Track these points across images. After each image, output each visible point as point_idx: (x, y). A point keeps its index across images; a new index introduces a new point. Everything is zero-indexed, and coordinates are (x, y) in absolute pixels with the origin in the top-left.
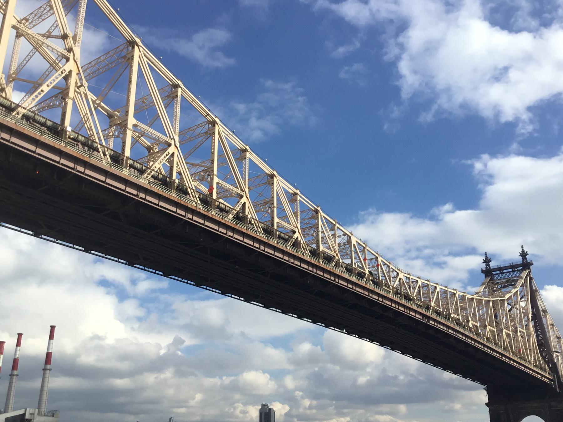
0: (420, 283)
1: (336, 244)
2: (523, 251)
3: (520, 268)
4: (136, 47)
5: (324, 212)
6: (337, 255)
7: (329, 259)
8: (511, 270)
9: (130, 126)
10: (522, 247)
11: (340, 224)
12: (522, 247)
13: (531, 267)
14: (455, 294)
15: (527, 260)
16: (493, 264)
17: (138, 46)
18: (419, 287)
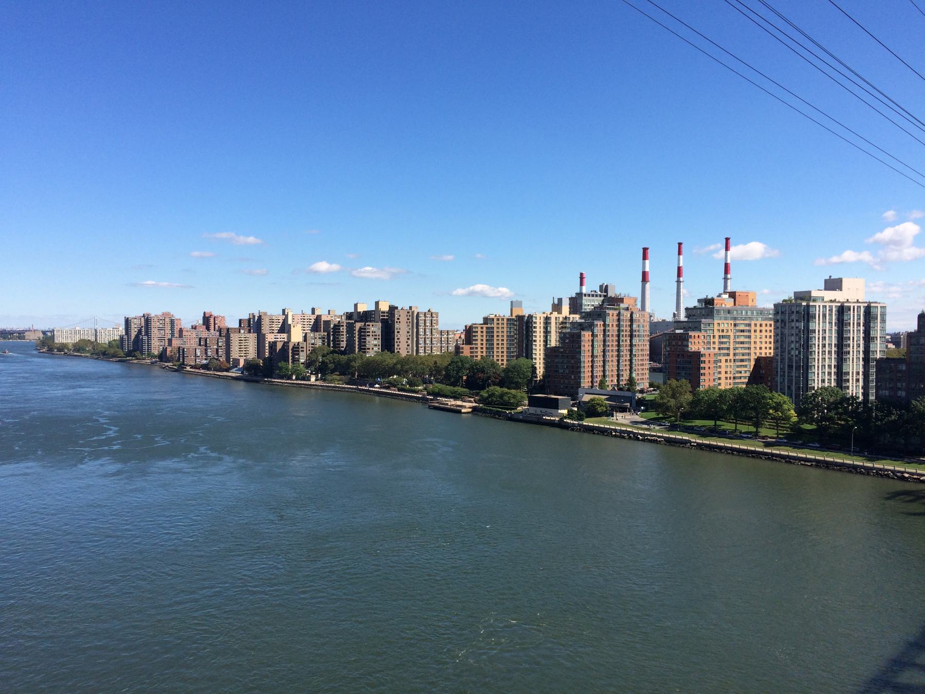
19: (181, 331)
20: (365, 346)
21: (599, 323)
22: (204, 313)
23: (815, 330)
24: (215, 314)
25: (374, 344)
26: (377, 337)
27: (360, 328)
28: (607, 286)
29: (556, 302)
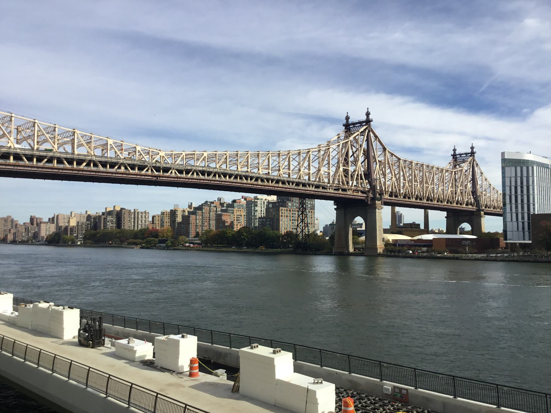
3: (364, 124)
8: (359, 125)
10: (368, 109)
12: (368, 109)
19: (16, 225)
20: (106, 227)
21: (200, 212)
22: (31, 216)
23: (257, 211)
24: (37, 216)
25: (111, 225)
26: (113, 223)
27: (104, 218)
28: (220, 199)
29: (190, 204)
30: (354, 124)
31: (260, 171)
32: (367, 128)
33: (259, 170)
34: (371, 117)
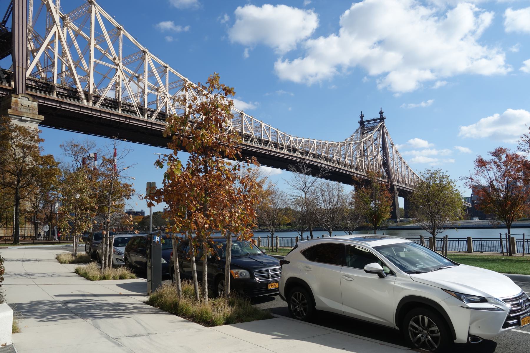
0: (303, 141)
1: (252, 128)
2: (381, 111)
4: (146, 54)
5: (245, 113)
6: (253, 134)
7: (248, 137)
8: (373, 122)
9: (146, 93)
10: (381, 108)
11: (255, 118)
12: (381, 108)
13: (385, 120)
14: (326, 143)
15: (382, 116)
16: (365, 119)
17: (147, 53)
18: (303, 143)
30: (368, 121)
31: (334, 158)
32: (382, 125)
33: (333, 156)
34: (384, 115)
